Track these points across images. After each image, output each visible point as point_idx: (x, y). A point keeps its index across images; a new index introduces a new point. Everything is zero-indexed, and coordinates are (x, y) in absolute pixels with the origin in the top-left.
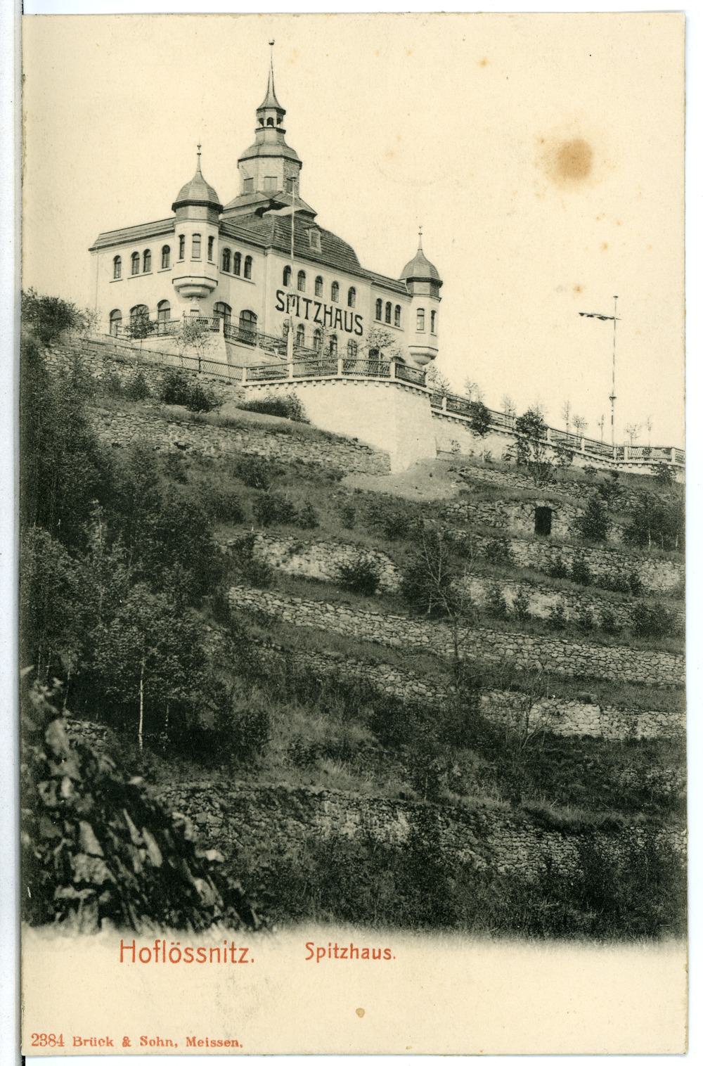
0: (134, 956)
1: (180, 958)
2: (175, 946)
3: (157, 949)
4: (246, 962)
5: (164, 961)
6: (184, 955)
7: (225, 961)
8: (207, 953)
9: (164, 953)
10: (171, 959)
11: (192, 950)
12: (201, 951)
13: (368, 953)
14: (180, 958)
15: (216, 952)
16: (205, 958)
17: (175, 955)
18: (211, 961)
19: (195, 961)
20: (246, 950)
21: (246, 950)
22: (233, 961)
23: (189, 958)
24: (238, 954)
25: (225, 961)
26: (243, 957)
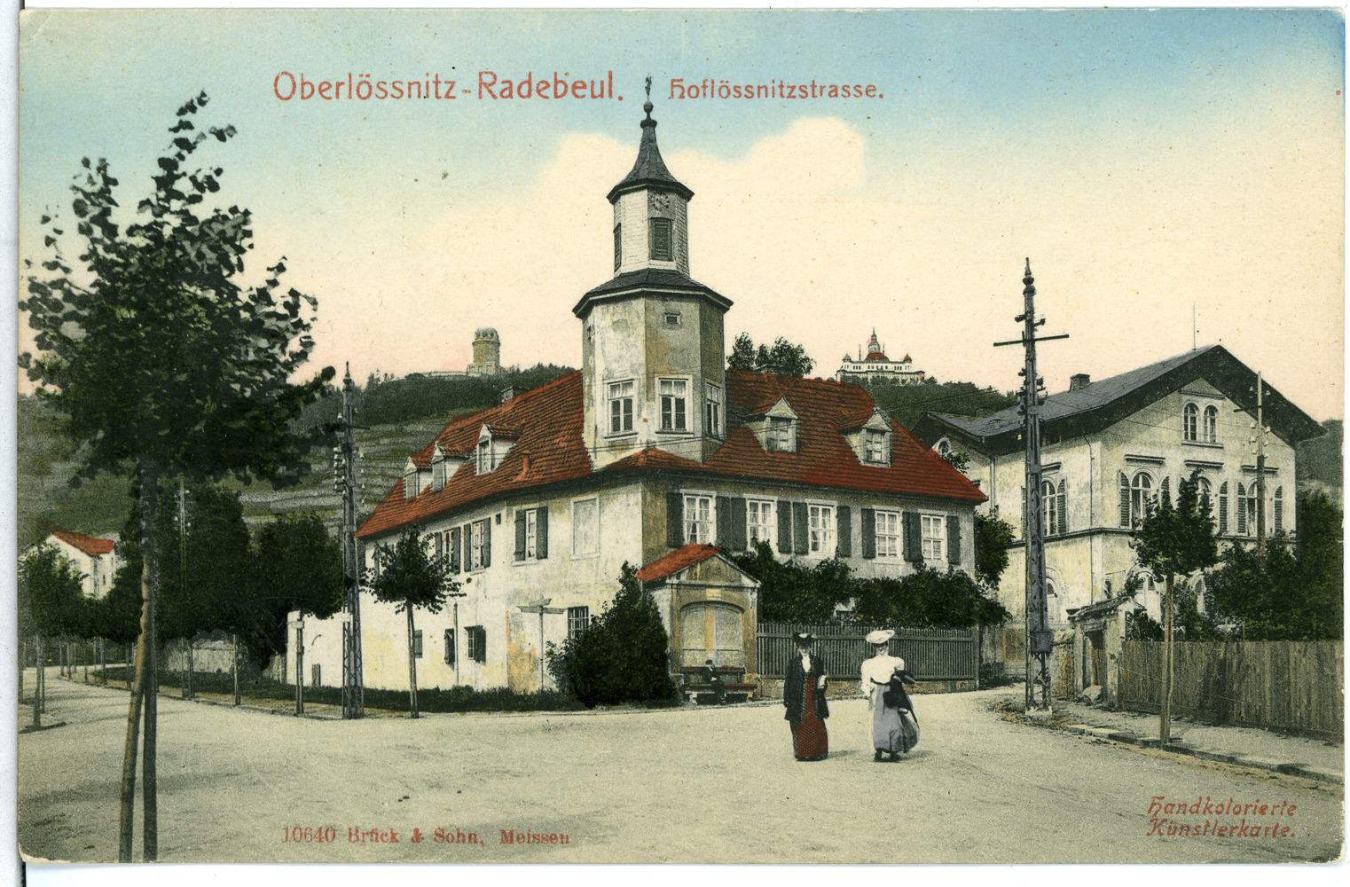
0: (350, 94)
1: (370, 93)
2: (364, 78)
4: (454, 97)
6: (375, 90)
8: (405, 88)
10: (359, 96)
11: (385, 83)
12: (397, 85)
14: (370, 93)
15: (416, 86)
16: (402, 92)
17: (364, 90)
19: (389, 96)
20: (453, 83)
21: (453, 83)
22: (438, 97)
23: (383, 94)
24: (443, 89)
26: (450, 89)
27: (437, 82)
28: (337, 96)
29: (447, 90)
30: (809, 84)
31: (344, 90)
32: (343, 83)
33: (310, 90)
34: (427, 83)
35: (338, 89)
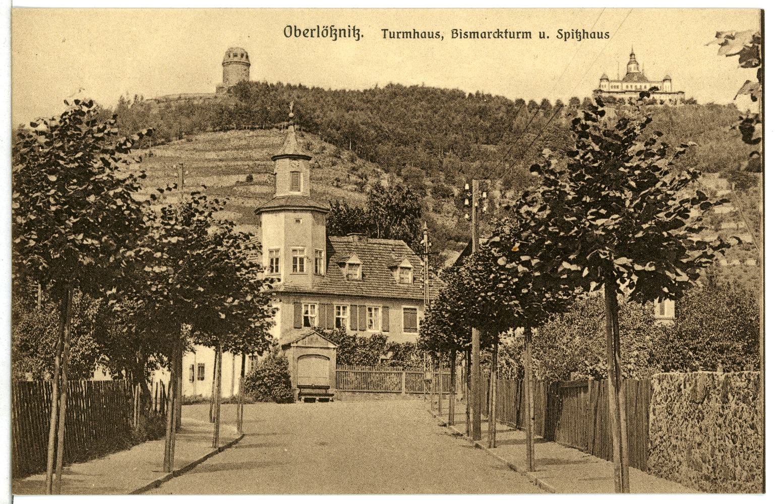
5: (318, 36)
7: (349, 36)
21: (359, 30)
25: (349, 36)
27: (354, 30)
28: (312, 36)
30: (504, 31)
31: (315, 33)
32: (315, 30)
34: (349, 30)
35: (312, 33)
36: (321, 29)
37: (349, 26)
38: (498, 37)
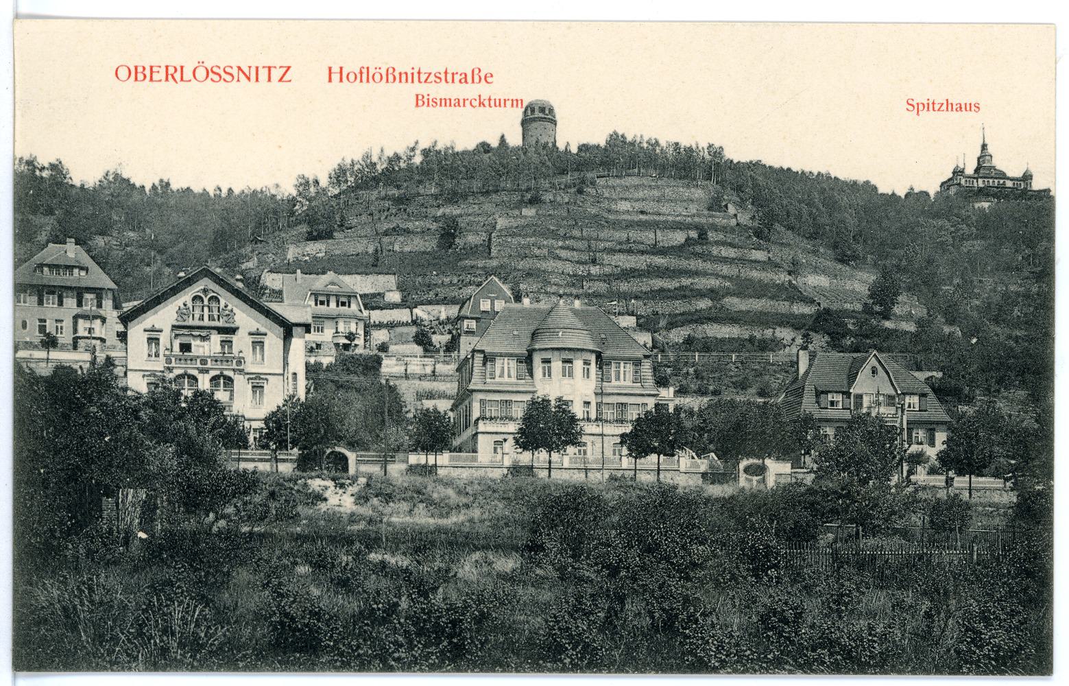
3: (361, 73)
7: (413, 82)
9: (368, 75)
13: (466, 78)
18: (400, 81)
22: (420, 81)
26: (428, 77)
29: (425, 78)
33: (350, 77)
34: (413, 74)
36: (372, 71)
37: (413, 68)
38: (167, 79)
